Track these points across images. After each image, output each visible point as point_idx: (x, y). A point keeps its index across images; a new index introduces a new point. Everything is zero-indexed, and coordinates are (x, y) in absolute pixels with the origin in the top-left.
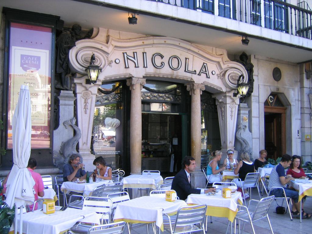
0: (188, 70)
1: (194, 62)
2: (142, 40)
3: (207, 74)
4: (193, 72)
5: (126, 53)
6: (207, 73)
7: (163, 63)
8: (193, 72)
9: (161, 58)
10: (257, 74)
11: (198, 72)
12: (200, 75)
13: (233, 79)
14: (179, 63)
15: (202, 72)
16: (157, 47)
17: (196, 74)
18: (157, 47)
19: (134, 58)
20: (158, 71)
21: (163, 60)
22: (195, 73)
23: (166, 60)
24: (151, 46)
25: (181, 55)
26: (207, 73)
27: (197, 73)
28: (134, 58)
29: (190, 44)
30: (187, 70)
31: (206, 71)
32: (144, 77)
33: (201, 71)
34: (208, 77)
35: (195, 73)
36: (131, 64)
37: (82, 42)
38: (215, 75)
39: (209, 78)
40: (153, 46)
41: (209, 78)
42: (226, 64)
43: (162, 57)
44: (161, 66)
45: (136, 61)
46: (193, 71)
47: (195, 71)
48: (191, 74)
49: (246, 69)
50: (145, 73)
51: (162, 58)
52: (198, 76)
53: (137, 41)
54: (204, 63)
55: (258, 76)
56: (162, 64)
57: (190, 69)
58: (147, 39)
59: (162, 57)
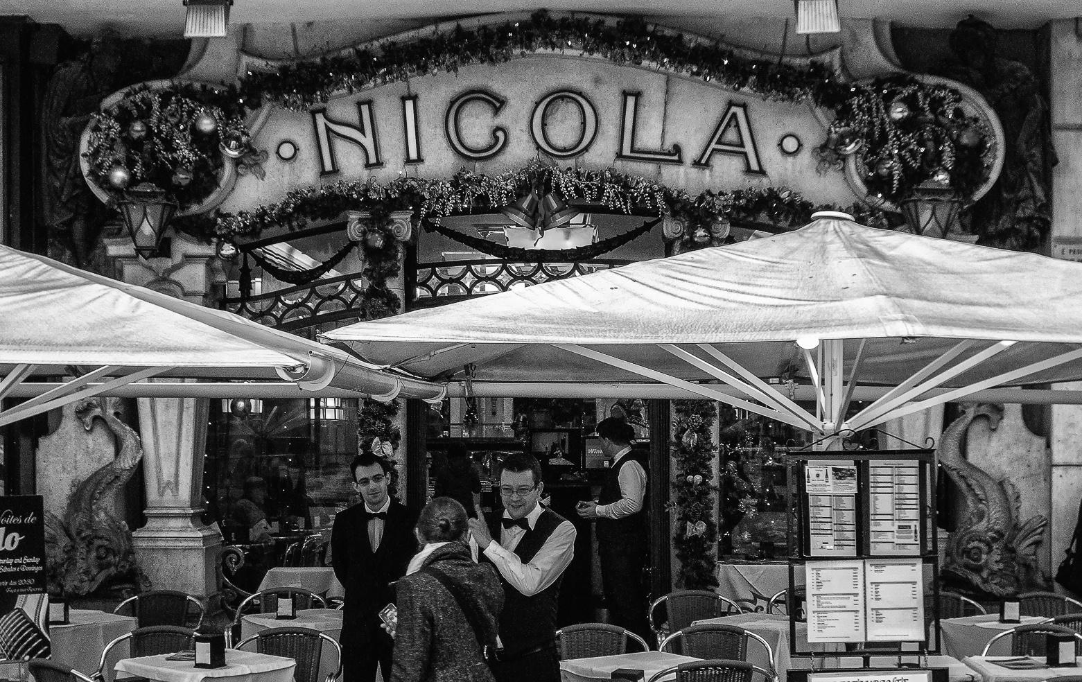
0: (632, 151)
3: (745, 154)
4: (669, 154)
6: (749, 148)
7: (500, 134)
8: (669, 154)
9: (490, 114)
11: (691, 153)
12: (707, 165)
14: (584, 123)
15: (714, 150)
17: (680, 162)
19: (362, 130)
21: (504, 119)
22: (676, 158)
25: (597, 81)
26: (749, 148)
27: (691, 153)
28: (362, 130)
30: (626, 152)
31: (742, 145)
33: (713, 145)
34: (754, 166)
35: (676, 158)
43: (497, 104)
44: (491, 147)
45: (368, 142)
46: (668, 146)
47: (677, 149)
49: (991, 105)
51: (497, 111)
52: (694, 172)
54: (731, 104)
56: (497, 139)
57: (650, 138)
59: (497, 104)
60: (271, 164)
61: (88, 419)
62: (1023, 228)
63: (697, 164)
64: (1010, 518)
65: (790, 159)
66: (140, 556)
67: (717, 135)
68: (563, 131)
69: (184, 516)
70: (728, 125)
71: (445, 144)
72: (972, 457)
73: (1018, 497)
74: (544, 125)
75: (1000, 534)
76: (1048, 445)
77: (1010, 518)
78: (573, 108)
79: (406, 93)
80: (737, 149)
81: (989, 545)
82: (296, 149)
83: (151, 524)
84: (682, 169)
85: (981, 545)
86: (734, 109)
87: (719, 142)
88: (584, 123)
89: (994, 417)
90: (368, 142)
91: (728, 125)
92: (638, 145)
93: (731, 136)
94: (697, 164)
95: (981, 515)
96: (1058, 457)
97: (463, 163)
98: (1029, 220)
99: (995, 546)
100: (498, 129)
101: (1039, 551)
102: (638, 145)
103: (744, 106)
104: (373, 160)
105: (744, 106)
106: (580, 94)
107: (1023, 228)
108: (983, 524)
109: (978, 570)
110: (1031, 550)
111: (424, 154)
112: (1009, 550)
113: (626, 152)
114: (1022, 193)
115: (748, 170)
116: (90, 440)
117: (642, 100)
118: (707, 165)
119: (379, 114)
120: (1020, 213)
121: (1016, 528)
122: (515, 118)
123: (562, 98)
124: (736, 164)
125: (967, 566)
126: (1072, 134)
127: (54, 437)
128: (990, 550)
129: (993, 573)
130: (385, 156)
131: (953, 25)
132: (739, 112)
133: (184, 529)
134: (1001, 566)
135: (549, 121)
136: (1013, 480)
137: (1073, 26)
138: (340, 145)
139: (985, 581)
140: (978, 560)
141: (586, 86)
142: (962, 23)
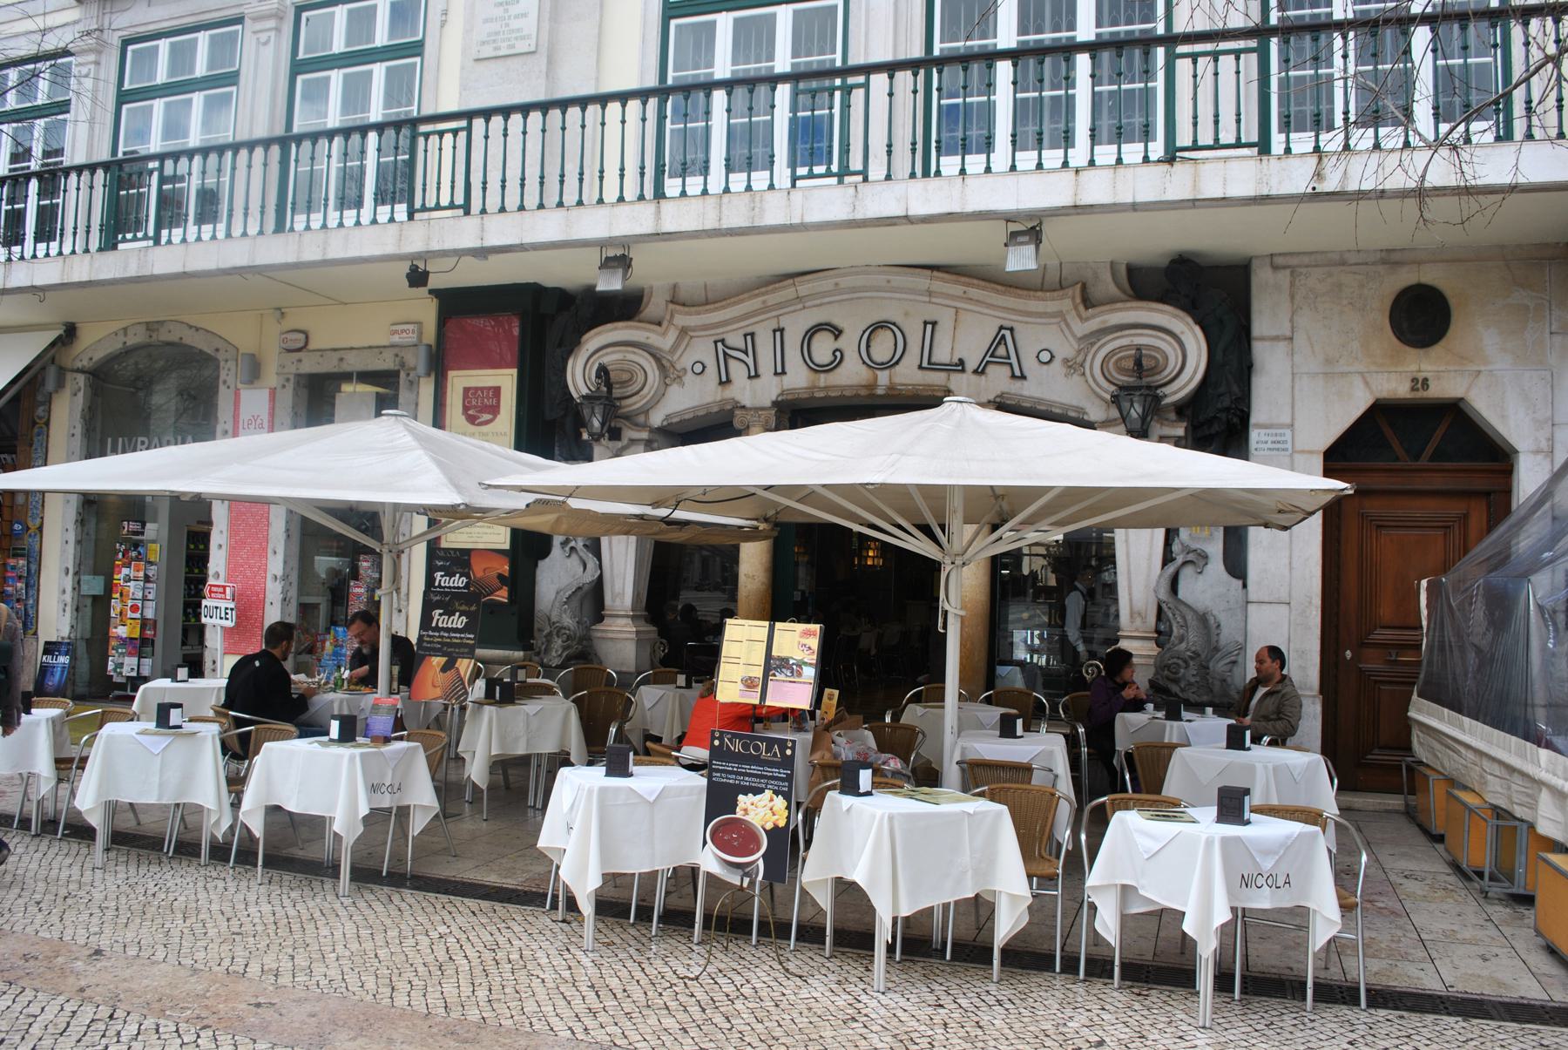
0: (929, 363)
1: (958, 331)
2: (757, 296)
3: (1011, 364)
4: (956, 365)
5: (723, 341)
6: (1014, 360)
7: (838, 354)
8: (956, 365)
9: (832, 338)
10: (1288, 334)
11: (971, 364)
12: (983, 372)
13: (1121, 370)
14: (896, 345)
16: (821, 305)
17: (963, 371)
18: (821, 305)
20: (823, 380)
21: (841, 343)
23: (849, 343)
24: (800, 306)
25: (906, 314)
26: (1014, 360)
27: (971, 364)
28: (746, 353)
29: (928, 272)
30: (925, 364)
31: (1009, 358)
32: (775, 404)
33: (987, 358)
34: (1018, 373)
36: (738, 371)
37: (599, 333)
38: (1057, 363)
39: (1023, 377)
40: (807, 304)
41: (1023, 377)
42: (1093, 317)
43: (837, 333)
46: (955, 360)
47: (961, 362)
48: (943, 375)
50: (779, 391)
51: (837, 337)
52: (974, 378)
53: (742, 301)
54: (1001, 328)
55: (1291, 339)
57: (942, 355)
58: (773, 291)
59: (837, 333)
60: (689, 378)
61: (567, 549)
62: (1223, 416)
63: (976, 372)
64: (1209, 641)
65: (1045, 367)
66: (595, 642)
67: (991, 352)
68: (882, 348)
69: (627, 616)
70: (999, 343)
71: (802, 361)
72: (1181, 595)
73: (1219, 626)
74: (868, 346)
75: (1196, 655)
76: (1245, 586)
77: (1209, 641)
78: (889, 333)
79: (776, 327)
80: (1005, 361)
81: (1185, 662)
82: (704, 367)
83: (606, 621)
84: (964, 376)
85: (1180, 662)
86: (1003, 332)
87: (992, 356)
88: (896, 345)
89: (1202, 563)
90: (750, 361)
91: (999, 343)
92: (934, 359)
93: (1001, 351)
94: (976, 372)
95: (1182, 639)
96: (1252, 597)
97: (812, 375)
98: (1227, 409)
99: (1191, 663)
100: (837, 350)
101: (1235, 669)
102: (934, 359)
103: (1012, 330)
104: (753, 373)
105: (1012, 330)
106: (894, 324)
107: (1223, 416)
108: (1183, 645)
109: (1176, 681)
110: (1227, 668)
111: (787, 370)
112: (1204, 668)
113: (925, 364)
114: (1222, 389)
115: (1013, 376)
116: (569, 561)
117: (938, 328)
118: (983, 372)
119: (758, 340)
120: (1219, 406)
121: (1217, 649)
122: (849, 343)
123: (882, 327)
124: (1006, 370)
125: (1168, 678)
126: (1267, 344)
127: (547, 560)
128: (1187, 667)
129: (1190, 684)
130: (761, 371)
131: (1165, 262)
132: (1007, 333)
133: (626, 626)
134: (1198, 679)
135: (873, 344)
136: (1215, 612)
137: (1268, 260)
138: (732, 363)
139: (1182, 690)
140: (1175, 673)
141: (899, 320)
142: (1173, 262)
